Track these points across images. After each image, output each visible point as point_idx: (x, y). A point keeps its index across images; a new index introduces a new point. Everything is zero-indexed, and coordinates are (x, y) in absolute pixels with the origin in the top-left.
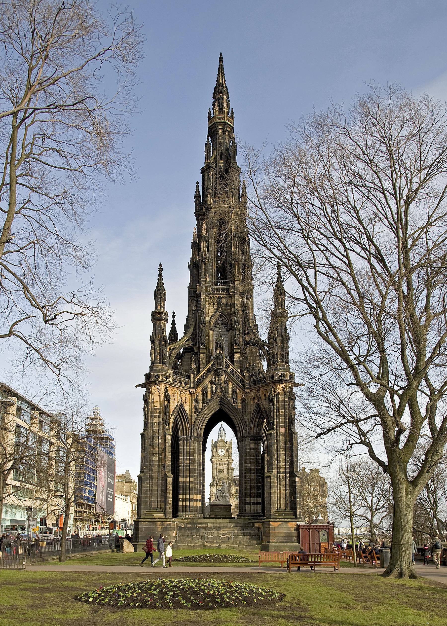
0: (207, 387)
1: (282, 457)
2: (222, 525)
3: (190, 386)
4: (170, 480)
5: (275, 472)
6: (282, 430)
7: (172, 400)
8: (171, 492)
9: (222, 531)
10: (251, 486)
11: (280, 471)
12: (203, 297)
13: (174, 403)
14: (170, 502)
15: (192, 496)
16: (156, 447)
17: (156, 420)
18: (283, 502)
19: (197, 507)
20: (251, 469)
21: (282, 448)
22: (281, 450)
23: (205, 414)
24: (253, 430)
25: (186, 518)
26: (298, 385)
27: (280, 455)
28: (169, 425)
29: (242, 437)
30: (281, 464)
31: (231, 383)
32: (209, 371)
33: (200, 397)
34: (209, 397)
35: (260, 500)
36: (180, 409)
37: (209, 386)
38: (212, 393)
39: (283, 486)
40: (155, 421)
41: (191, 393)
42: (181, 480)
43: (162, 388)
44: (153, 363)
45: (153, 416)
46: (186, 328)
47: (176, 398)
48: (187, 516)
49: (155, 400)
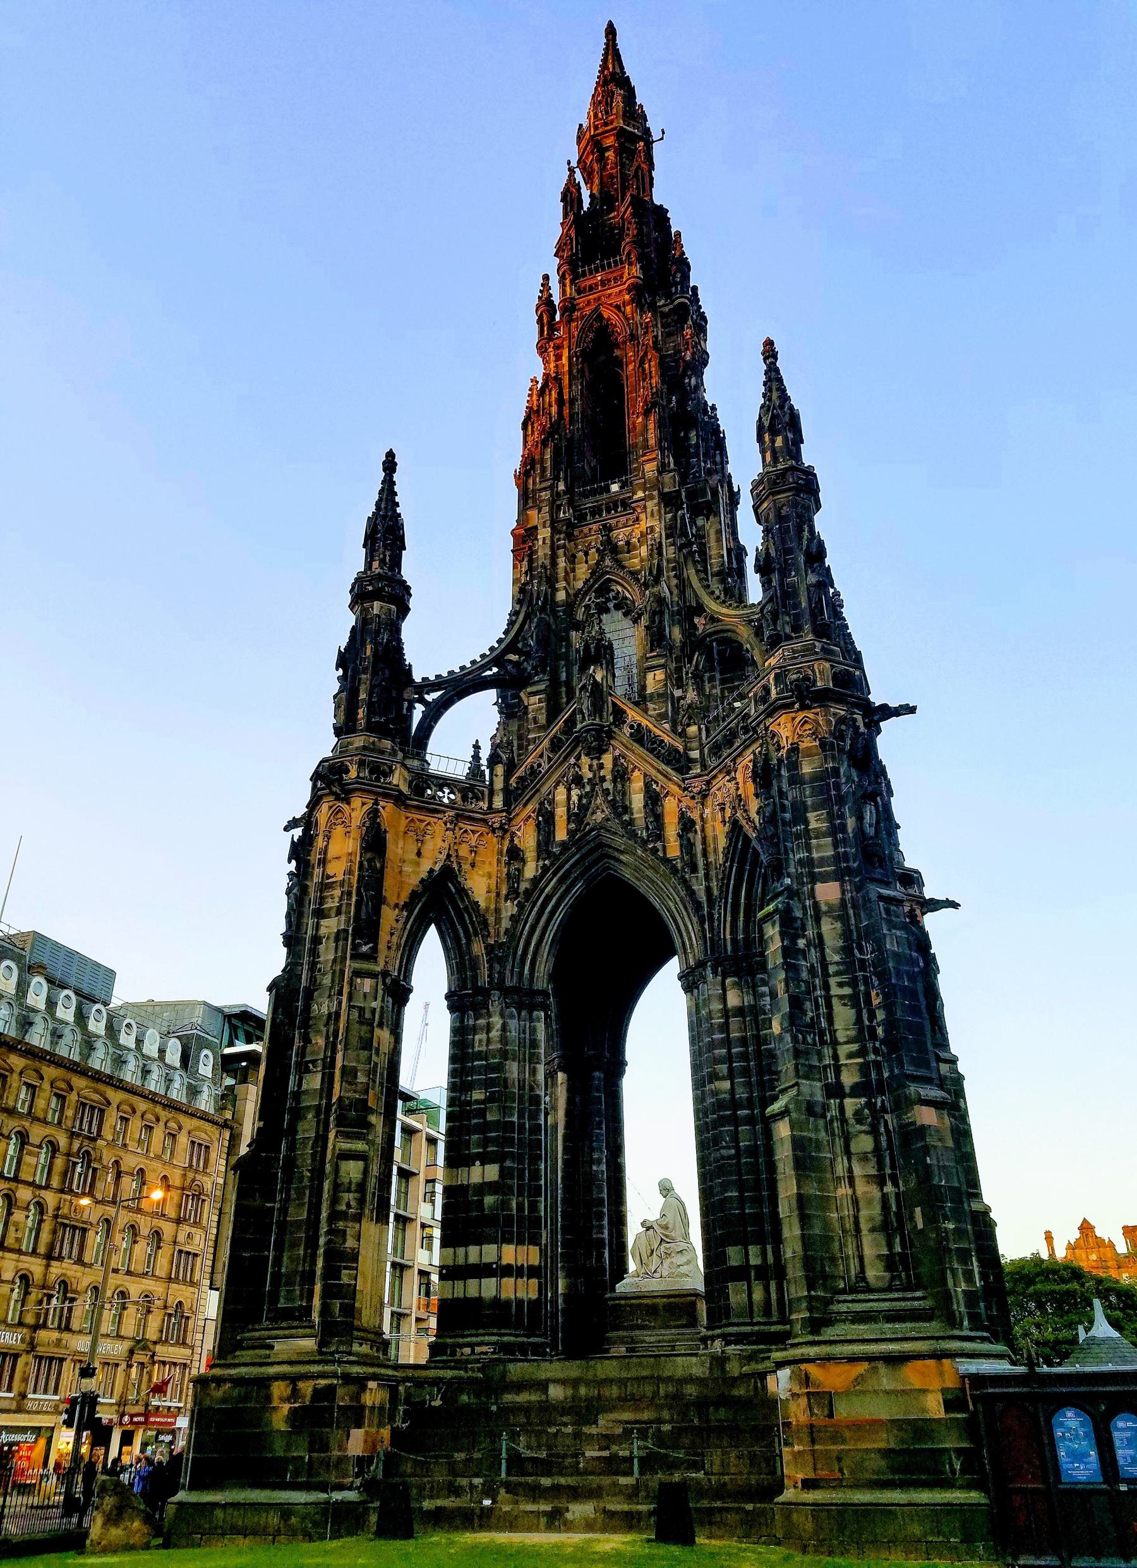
0: (552, 802)
1: (844, 1017)
3: (491, 803)
6: (828, 892)
11: (839, 1085)
13: (418, 864)
16: (318, 1032)
17: (330, 926)
18: (872, 1247)
20: (734, 1104)
21: (837, 974)
22: (833, 981)
23: (548, 898)
24: (734, 931)
25: (461, 1364)
27: (829, 1006)
28: (374, 938)
30: (843, 1050)
32: (555, 745)
33: (527, 839)
34: (561, 835)
39: (864, 1158)
40: (323, 931)
43: (357, 809)
45: (320, 914)
48: (467, 1350)
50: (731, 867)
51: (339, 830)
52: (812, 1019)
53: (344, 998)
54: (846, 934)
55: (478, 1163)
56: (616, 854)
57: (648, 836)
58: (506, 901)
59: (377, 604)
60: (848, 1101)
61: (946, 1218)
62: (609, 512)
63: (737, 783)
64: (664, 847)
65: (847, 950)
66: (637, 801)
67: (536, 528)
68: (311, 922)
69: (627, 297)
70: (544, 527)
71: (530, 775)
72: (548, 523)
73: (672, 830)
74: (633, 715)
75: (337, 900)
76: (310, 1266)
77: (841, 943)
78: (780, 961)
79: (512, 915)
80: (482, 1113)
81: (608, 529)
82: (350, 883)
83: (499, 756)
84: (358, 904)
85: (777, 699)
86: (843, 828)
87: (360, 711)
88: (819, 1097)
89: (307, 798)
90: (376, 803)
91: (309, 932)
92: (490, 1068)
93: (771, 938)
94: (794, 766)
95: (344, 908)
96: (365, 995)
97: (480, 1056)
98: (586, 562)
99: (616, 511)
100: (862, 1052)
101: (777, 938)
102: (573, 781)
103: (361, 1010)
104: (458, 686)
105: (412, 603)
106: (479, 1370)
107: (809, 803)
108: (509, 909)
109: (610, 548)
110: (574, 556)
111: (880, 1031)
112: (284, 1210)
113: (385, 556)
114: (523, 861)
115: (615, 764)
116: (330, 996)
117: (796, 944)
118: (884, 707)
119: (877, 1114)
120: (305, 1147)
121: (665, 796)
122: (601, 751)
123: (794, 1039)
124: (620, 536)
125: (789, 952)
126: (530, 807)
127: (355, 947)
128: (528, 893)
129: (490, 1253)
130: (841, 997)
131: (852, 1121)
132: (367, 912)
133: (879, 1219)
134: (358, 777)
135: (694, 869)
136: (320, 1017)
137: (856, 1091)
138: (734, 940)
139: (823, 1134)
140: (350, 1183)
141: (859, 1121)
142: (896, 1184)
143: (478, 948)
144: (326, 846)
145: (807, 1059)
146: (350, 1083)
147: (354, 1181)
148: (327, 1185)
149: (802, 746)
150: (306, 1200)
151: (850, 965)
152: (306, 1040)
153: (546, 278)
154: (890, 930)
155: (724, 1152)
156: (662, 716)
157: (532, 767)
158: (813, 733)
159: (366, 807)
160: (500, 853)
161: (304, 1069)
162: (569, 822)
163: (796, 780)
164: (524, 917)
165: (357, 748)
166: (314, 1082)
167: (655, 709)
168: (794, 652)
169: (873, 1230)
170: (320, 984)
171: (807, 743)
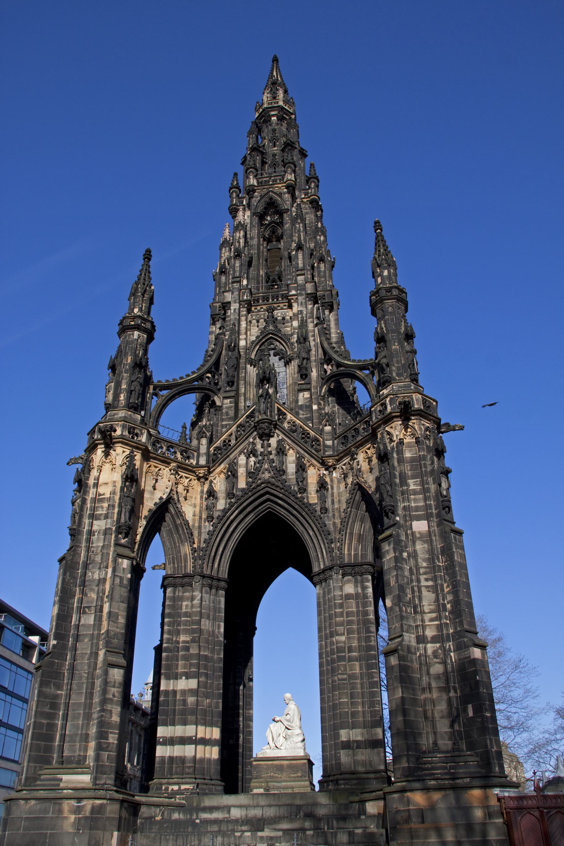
0: (236, 464)
1: (428, 598)
6: (420, 526)
10: (352, 696)
12: (235, 306)
13: (153, 494)
14: (113, 739)
16: (92, 590)
19: (209, 760)
21: (425, 573)
22: (422, 578)
24: (349, 550)
27: (420, 591)
29: (324, 571)
30: (427, 617)
31: (291, 451)
34: (242, 484)
37: (242, 460)
40: (95, 528)
41: (199, 479)
43: (120, 453)
45: (93, 517)
48: (176, 788)
49: (101, 481)
50: (351, 511)
51: (107, 467)
52: (410, 598)
53: (110, 570)
54: (431, 551)
55: (184, 678)
56: (276, 500)
57: (299, 489)
58: (205, 522)
59: (136, 333)
60: (429, 645)
61: (486, 710)
62: (273, 300)
63: (358, 462)
64: (308, 497)
65: (431, 560)
66: (291, 468)
67: (229, 303)
68: (86, 521)
69: (286, 190)
70: (235, 302)
71: (224, 445)
72: (237, 301)
74: (289, 416)
75: (105, 509)
76: (86, 730)
77: (427, 556)
78: (393, 564)
79: (209, 531)
80: (187, 649)
81: (271, 310)
82: (114, 500)
83: (204, 433)
84: (120, 513)
85: (391, 413)
86: (428, 490)
87: (122, 395)
88: (413, 643)
89: (85, 445)
90: (132, 452)
91: (86, 528)
92: (193, 623)
93: (388, 551)
94: (400, 452)
95: (110, 515)
96: (124, 569)
97: (186, 614)
98: (258, 326)
99: (277, 300)
100: (439, 618)
101: (392, 551)
102: (251, 452)
103: (121, 579)
104: (179, 389)
105: (156, 335)
106: (183, 799)
107: (410, 474)
108: (208, 527)
110: (250, 322)
111: (449, 606)
112: (69, 696)
113: (142, 306)
114: (217, 498)
115: (278, 445)
116: (100, 568)
117: (402, 556)
118: (447, 424)
119: (446, 652)
120: (83, 658)
121: (309, 466)
122: (270, 436)
123: (401, 610)
124: (278, 314)
125: (398, 559)
126: (222, 466)
128: (220, 518)
129: (189, 730)
130: (427, 587)
131: (431, 657)
132: (125, 519)
133: (445, 712)
134: (122, 434)
136: (94, 580)
137: (434, 640)
138: (350, 555)
139: (415, 663)
140: (115, 682)
141: (435, 657)
142: (456, 692)
143: (186, 549)
144: (99, 476)
145: (407, 621)
146: (114, 622)
147: (117, 681)
148: (98, 682)
149: (405, 441)
150: (84, 691)
151: (433, 568)
152: (83, 593)
153: (236, 174)
154: (456, 549)
155: (340, 676)
156: (307, 419)
157: (225, 441)
158: (412, 434)
159: (125, 454)
160: (202, 492)
161: (82, 611)
162: (247, 476)
163: (401, 460)
164: (216, 533)
165: (120, 417)
166: (90, 619)
167: (303, 415)
168: (400, 387)
169: (442, 717)
170: (93, 560)
171: (407, 440)
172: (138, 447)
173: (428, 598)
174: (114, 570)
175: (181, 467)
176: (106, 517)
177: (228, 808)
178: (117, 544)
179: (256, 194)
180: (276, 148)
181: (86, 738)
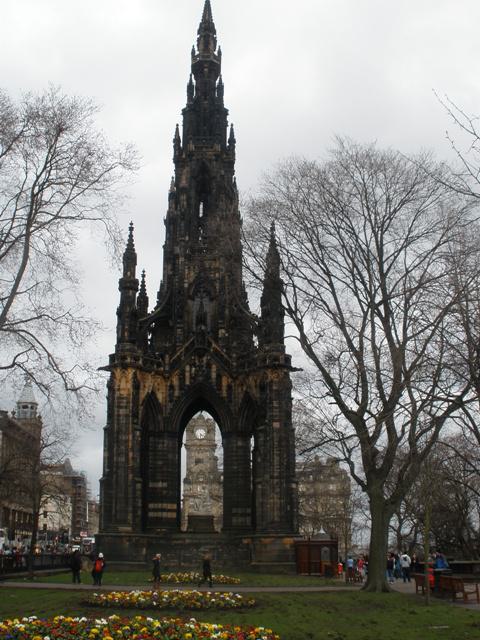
1: (276, 459)
2: (203, 541)
4: (139, 486)
5: (267, 477)
7: (142, 387)
8: (140, 501)
9: (202, 549)
12: (181, 260)
14: (139, 513)
15: (165, 505)
17: (122, 412)
26: (295, 369)
28: (137, 417)
33: (176, 381)
35: (249, 511)
36: (152, 396)
38: (191, 378)
41: (164, 378)
42: (151, 485)
44: (120, 340)
45: (119, 407)
46: (160, 295)
47: (147, 385)
49: (121, 387)
51: (124, 380)
53: (131, 437)
65: (280, 441)
66: (214, 375)
68: (116, 409)
73: (224, 388)
91: (116, 413)
94: (271, 386)
108: (170, 405)
109: (203, 269)
119: (281, 483)
122: (204, 355)
124: (207, 265)
127: (133, 420)
135: (230, 401)
137: (277, 478)
148: (130, 489)
151: (280, 445)
152: (118, 447)
161: (119, 455)
163: (271, 390)
172: (138, 368)
173: (276, 459)
174: (133, 437)
175: (157, 373)
176: (126, 407)
177: (184, 539)
178: (133, 423)
179: (194, 158)
180: (206, 102)
181: (127, 512)
